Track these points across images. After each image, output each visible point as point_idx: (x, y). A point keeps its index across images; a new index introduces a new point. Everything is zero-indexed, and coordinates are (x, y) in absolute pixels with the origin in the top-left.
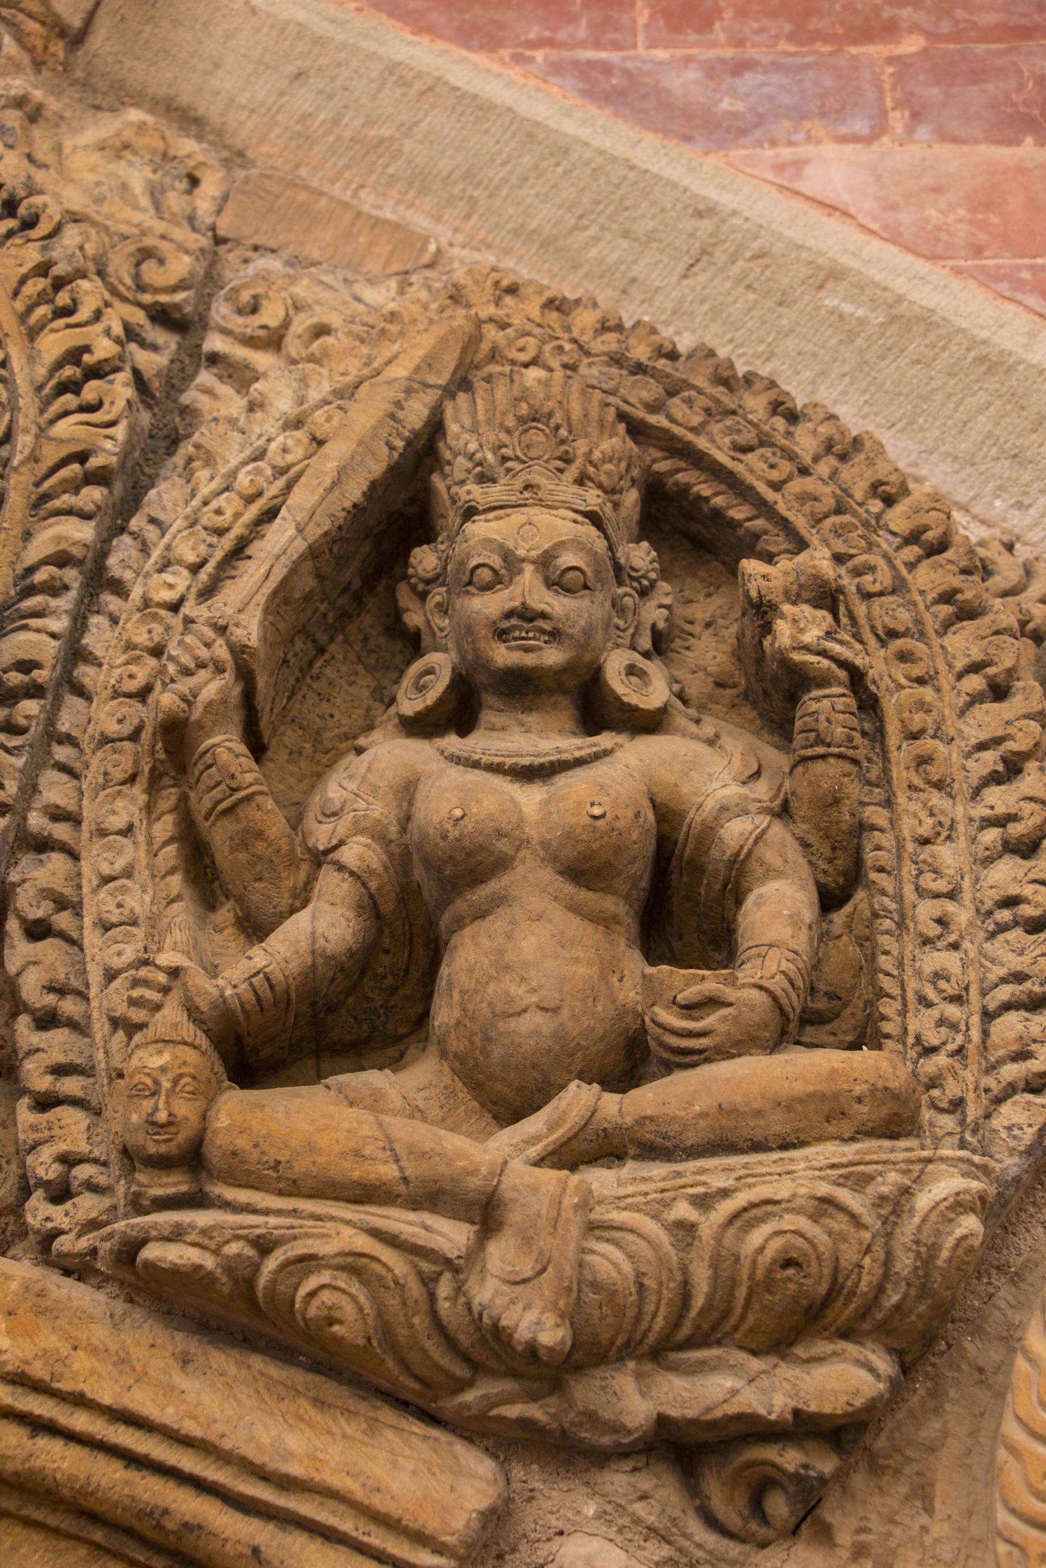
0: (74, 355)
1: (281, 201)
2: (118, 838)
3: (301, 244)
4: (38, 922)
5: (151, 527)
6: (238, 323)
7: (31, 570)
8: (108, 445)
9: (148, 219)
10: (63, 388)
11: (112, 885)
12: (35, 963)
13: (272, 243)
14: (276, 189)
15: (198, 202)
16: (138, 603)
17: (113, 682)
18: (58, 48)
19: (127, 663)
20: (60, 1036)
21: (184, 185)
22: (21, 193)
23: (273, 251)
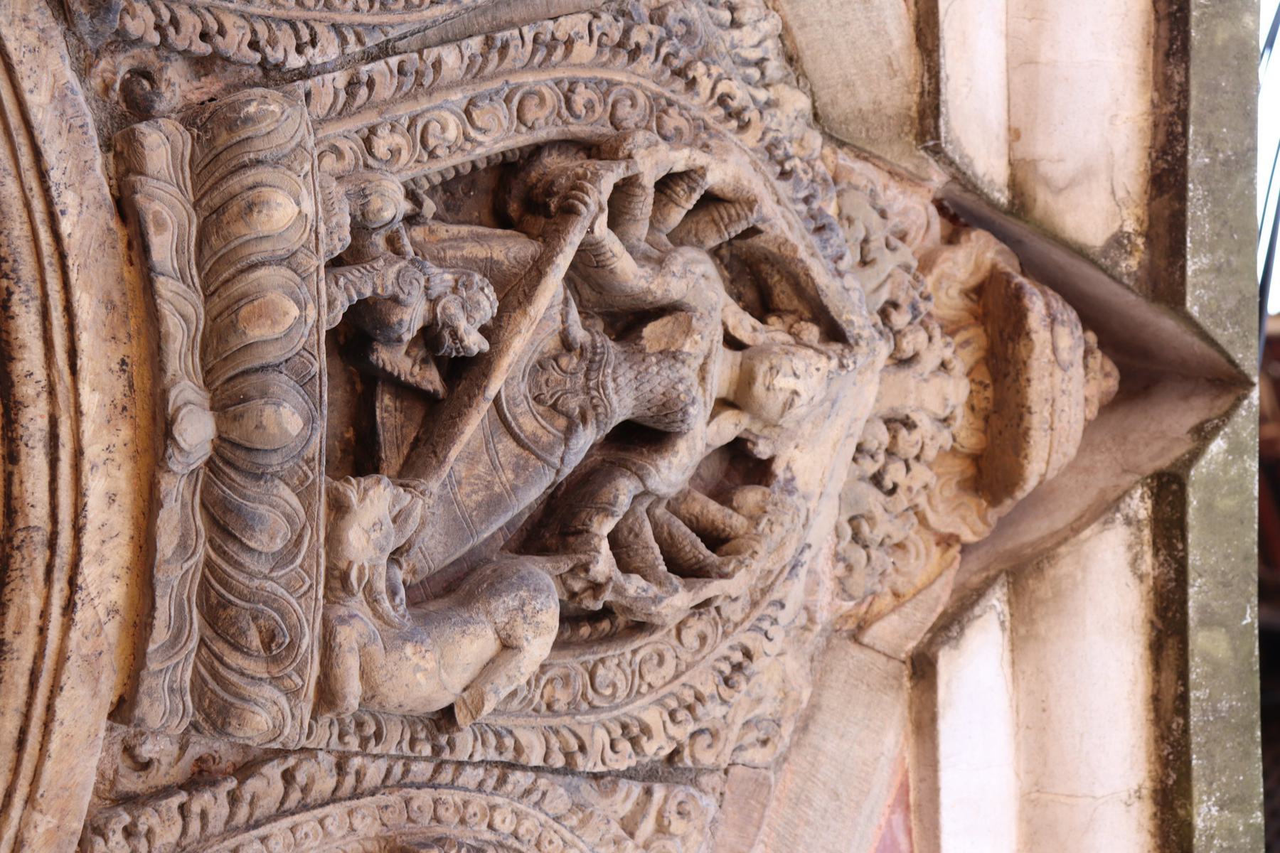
0: (646, 730)
4: (294, 778)
6: (672, 806)
7: (511, 732)
8: (590, 765)
9: (740, 721)
10: (624, 727)
11: (319, 827)
18: (851, 625)
21: (762, 736)
22: (747, 672)
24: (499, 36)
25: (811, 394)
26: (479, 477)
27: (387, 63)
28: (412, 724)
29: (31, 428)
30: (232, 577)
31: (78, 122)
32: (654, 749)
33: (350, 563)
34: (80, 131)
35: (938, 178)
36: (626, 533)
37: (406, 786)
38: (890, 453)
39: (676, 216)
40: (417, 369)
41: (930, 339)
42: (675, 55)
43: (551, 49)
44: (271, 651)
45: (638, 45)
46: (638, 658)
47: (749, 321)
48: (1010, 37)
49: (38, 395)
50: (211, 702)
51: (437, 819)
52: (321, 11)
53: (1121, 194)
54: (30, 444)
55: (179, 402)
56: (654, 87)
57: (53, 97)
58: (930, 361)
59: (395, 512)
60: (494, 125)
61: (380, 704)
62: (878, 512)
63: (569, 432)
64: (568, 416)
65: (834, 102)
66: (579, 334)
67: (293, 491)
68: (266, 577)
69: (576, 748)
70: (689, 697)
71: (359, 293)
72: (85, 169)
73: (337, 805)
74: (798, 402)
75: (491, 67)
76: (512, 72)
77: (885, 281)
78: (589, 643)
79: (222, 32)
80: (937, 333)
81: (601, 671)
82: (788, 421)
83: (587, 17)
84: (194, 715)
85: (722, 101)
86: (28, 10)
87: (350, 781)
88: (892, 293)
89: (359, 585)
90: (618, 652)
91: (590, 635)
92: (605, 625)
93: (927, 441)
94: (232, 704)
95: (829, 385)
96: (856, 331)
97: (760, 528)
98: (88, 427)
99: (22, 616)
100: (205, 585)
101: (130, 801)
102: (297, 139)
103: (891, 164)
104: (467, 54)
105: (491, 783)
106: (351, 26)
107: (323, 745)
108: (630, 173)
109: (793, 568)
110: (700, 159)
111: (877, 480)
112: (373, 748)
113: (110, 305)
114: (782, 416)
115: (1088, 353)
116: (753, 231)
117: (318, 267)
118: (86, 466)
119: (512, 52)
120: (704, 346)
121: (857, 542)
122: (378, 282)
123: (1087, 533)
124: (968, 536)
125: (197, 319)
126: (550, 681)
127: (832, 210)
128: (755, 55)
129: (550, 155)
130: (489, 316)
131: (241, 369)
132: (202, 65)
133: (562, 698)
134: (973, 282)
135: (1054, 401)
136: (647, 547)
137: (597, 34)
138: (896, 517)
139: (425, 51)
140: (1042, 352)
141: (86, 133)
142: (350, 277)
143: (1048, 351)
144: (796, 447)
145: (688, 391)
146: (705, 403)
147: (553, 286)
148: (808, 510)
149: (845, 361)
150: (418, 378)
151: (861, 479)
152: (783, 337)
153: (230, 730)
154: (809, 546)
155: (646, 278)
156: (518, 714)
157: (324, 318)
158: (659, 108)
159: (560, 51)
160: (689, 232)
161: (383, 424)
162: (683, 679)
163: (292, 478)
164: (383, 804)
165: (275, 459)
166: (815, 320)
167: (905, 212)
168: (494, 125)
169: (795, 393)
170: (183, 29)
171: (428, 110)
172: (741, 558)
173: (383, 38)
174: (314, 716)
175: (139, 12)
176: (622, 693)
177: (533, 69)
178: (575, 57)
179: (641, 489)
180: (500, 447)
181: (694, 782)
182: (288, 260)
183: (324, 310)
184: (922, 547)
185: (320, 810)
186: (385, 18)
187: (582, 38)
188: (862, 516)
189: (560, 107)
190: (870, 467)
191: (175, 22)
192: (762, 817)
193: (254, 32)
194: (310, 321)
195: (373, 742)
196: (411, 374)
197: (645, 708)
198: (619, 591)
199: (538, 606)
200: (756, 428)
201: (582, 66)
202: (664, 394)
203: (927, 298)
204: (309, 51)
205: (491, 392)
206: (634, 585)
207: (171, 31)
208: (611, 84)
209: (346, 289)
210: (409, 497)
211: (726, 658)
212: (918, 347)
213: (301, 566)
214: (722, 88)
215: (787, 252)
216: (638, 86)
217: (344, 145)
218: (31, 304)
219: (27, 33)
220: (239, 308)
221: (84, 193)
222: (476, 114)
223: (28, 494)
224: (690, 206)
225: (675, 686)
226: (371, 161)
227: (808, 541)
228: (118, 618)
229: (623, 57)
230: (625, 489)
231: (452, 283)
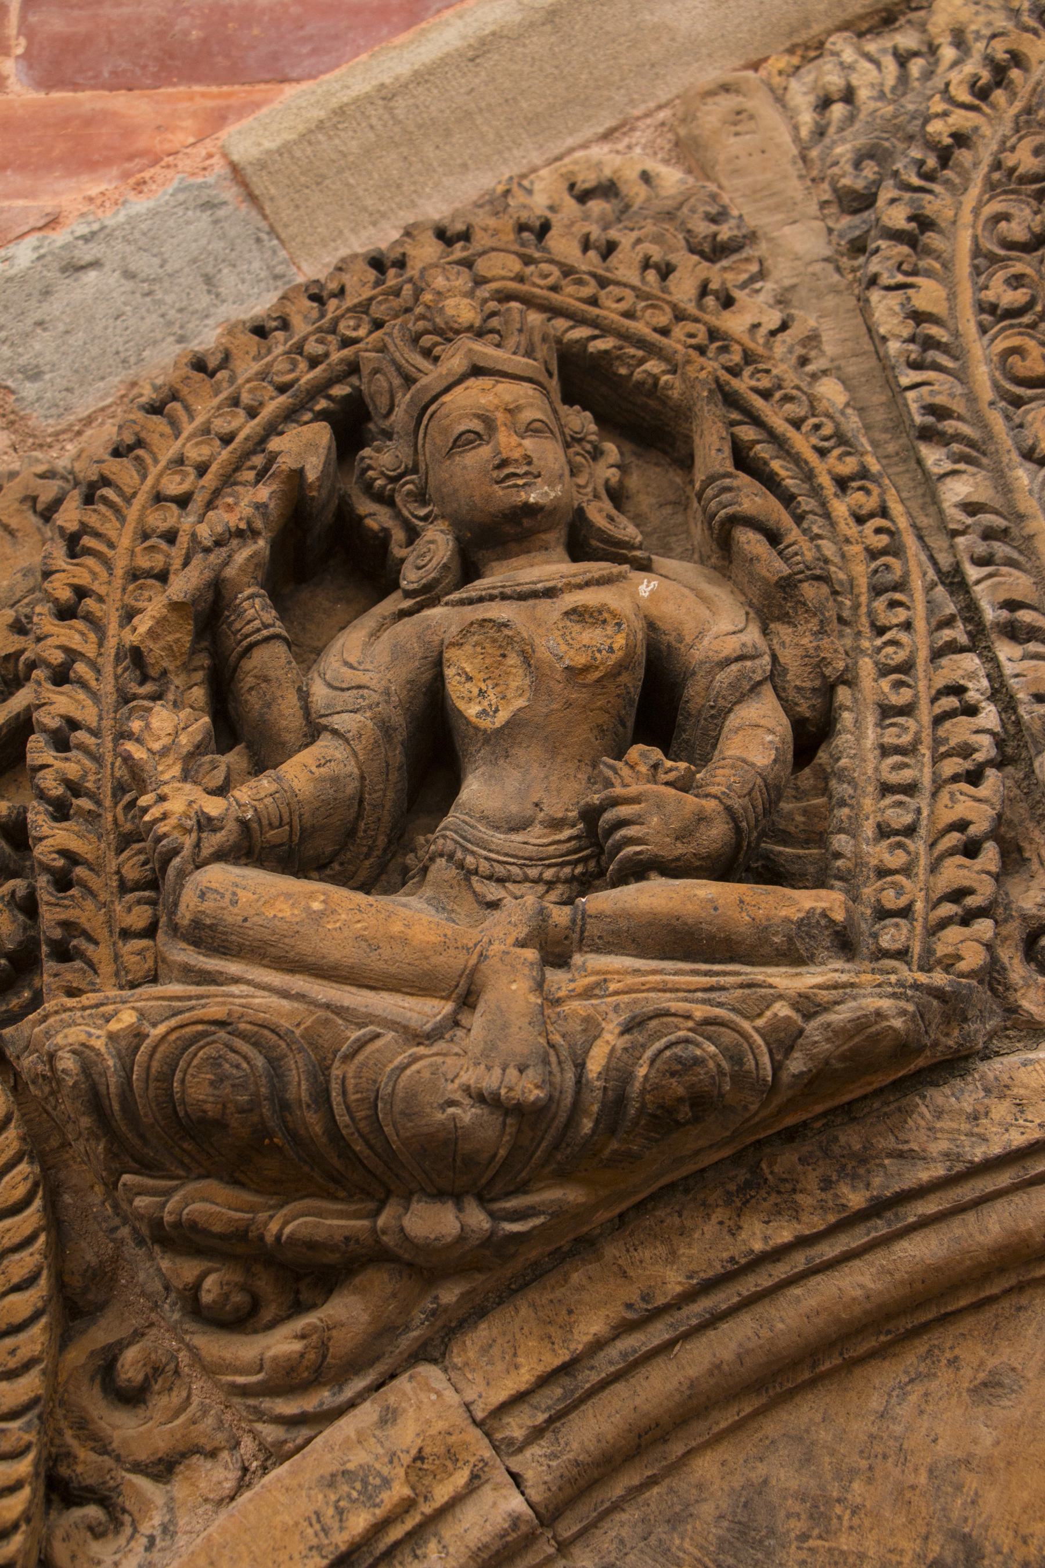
24: (918, 419)
27: (978, 582)
42: (921, 163)
43: (929, 343)
45: (911, 219)
52: (916, 679)
56: (975, 191)
75: (965, 429)
76: (971, 398)
79: (961, 826)
83: (875, 295)
85: (982, 93)
86: (961, 1111)
104: (948, 466)
119: (939, 400)
137: (900, 278)
159: (934, 330)
170: (966, 883)
175: (950, 950)
177: (964, 368)
178: (940, 309)
186: (917, 584)
187: (909, 299)
189: (1020, 325)
191: (957, 895)
193: (955, 778)
201: (952, 296)
204: (972, 696)
207: (970, 901)
208: (977, 251)
214: (965, 97)
216: (976, 212)
219: (995, 1115)
229: (931, 239)
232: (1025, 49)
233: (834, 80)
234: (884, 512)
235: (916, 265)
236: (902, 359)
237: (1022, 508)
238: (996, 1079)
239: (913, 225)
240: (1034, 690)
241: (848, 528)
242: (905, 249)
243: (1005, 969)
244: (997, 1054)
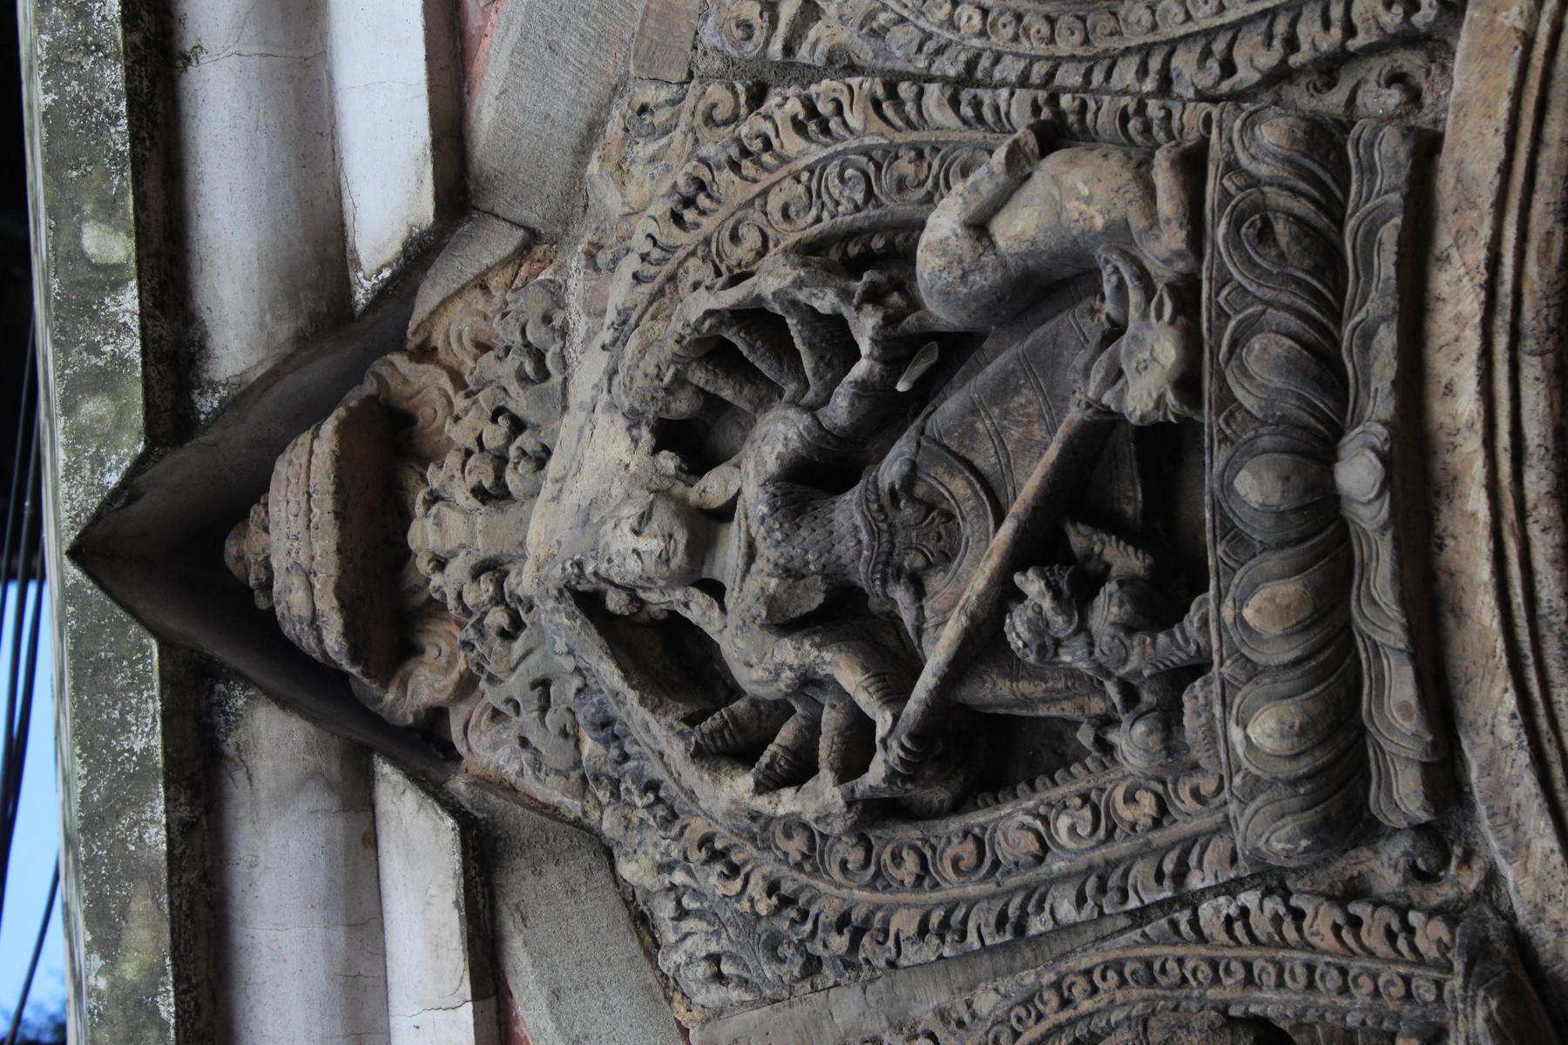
0: (799, 127)
1: (655, 38)
2: (1157, 13)
3: (689, 14)
5: (925, 49)
6: (759, 36)
7: (965, 121)
8: (866, 85)
9: (677, 134)
10: (825, 130)
11: (1192, 12)
12: (1252, 61)
13: (691, 36)
14: (646, 43)
15: (661, 100)
16: (983, 40)
17: (1043, 46)
18: (539, 251)
19: (1028, 38)
20: (1302, 30)
21: (647, 118)
22: (677, 197)
23: (697, 33)
24: (1008, 937)
25: (618, 532)
26: (1017, 423)
27: (1141, 901)
28: (1084, 130)
29: (1542, 469)
30: (1309, 302)
31: (1499, 820)
32: (788, 106)
33: (1172, 322)
34: (1496, 810)
35: (459, 785)
36: (836, 362)
37: (1088, 59)
38: (501, 461)
39: (787, 733)
40: (1097, 549)
41: (460, 596)
42: (793, 922)
43: (945, 924)
44: (1261, 218)
45: (840, 932)
46: (814, 212)
47: (694, 615)
48: (380, 953)
49: (1535, 507)
50: (1327, 157)
51: (1051, 21)
52: (1223, 958)
53: (240, 775)
54: (1543, 451)
55: (1377, 504)
56: (821, 886)
57: (1528, 847)
58: (458, 569)
59: (1121, 382)
60: (1014, 835)
61: (1130, 158)
62: (514, 388)
63: (911, 477)
64: (913, 500)
65: (589, 872)
66: (901, 595)
67: (1241, 405)
68: (1269, 303)
69: (885, 105)
70: (748, 167)
71: (1172, 636)
72: (1489, 766)
73: (1171, 36)
74: (634, 521)
75: (1016, 902)
76: (992, 897)
77: (518, 663)
78: (874, 229)
79: (1336, 929)
80: (451, 603)
81: (859, 197)
82: (642, 498)
83: (903, 962)
84: (1345, 141)
85: (734, 871)
86: (1556, 941)
87: (1155, 64)
88: (510, 649)
89: (1161, 297)
90: (839, 219)
91: (871, 238)
92: (853, 250)
93: (458, 474)
94: (1304, 155)
95: (596, 542)
96: (562, 607)
97: (672, 370)
98: (1478, 470)
99: (1544, 254)
100: (1340, 294)
101: (1409, 39)
102: (1249, 811)
103: (516, 802)
104: (1046, 915)
105: (985, 62)
106: (1185, 942)
107: (1191, 105)
108: (849, 784)
109: (624, 323)
110: (762, 803)
111: (518, 426)
112: (1129, 102)
113: (1459, 613)
114: (652, 504)
115: (267, 585)
116: (692, 720)
117: (1222, 663)
118: (1479, 426)
119: (992, 920)
120: (753, 585)
121: (537, 350)
122: (1149, 650)
123: (260, 372)
124: (399, 360)
125: (1359, 600)
126: (921, 184)
127: (588, 745)
128: (688, 925)
129: (941, 802)
130: (1016, 613)
131: (1308, 544)
132: (1355, 890)
133: (905, 166)
134: (410, 665)
135: (308, 527)
136: (811, 346)
137: (891, 943)
138: (491, 382)
139: (1096, 916)
140: (324, 585)
141: (1489, 807)
142: (1183, 656)
143: (318, 586)
144: (627, 466)
145: (770, 531)
146: (746, 517)
147: (937, 653)
148: (609, 391)
149: (576, 570)
150: (1095, 538)
151: (537, 427)
152: (652, 597)
153: (1303, 125)
154: (604, 347)
155: (824, 662)
156: (957, 145)
157: (1212, 606)
158: (813, 857)
159: (935, 920)
160: (769, 716)
161: (1133, 484)
162: (757, 188)
163: (1243, 419)
164: (1116, 38)
165: (1265, 442)
166: (612, 617)
167: (495, 747)
168: (1014, 835)
169: (637, 533)
170: (1382, 930)
171: (1092, 848)
172: (696, 335)
173: (1147, 929)
174: (1204, 144)
175: (1434, 947)
176: (832, 170)
177: (966, 900)
179: (820, 413)
180: (993, 460)
181: (729, 61)
182: (1253, 671)
183: (1212, 616)
184: (455, 345)
185: (1191, 30)
186: (1147, 952)
187: (908, 938)
188: (533, 382)
189: (933, 857)
190: (526, 440)
191: (1391, 937)
192: (643, 22)
193: (1299, 930)
194: (1229, 602)
195: (1131, 110)
196: (1104, 543)
197: (802, 153)
198: (845, 295)
199: (945, 275)
200: (679, 488)
201: (907, 906)
202: (799, 527)
203: (467, 645)
204: (1233, 911)
205: (1008, 528)
206: (826, 302)
207: (1395, 926)
208: (871, 886)
209: (1187, 641)
210: (1105, 400)
211: (702, 213)
212: (474, 586)
213: (1229, 317)
214: (737, 885)
215: (652, 699)
216: (839, 886)
217: (1190, 804)
218: (1546, 611)
219: (1558, 916)
220: (1311, 615)
221: (1490, 739)
222: (1035, 847)
223: (1543, 393)
224: (772, 748)
225: (766, 179)
226: (1159, 788)
227: (606, 354)
228: (1437, 252)
229: (857, 916)
230: (840, 409)
231: (1061, 651)
232: (698, 836)
233: (702, 970)
234: (1088, 973)
235: (879, 930)
236: (959, 946)
237: (1083, 867)
238: (1530, 913)
239: (845, 931)
240: (1227, 865)
241: (1102, 999)
242: (866, 940)
243: (1446, 902)
244: (1511, 907)
